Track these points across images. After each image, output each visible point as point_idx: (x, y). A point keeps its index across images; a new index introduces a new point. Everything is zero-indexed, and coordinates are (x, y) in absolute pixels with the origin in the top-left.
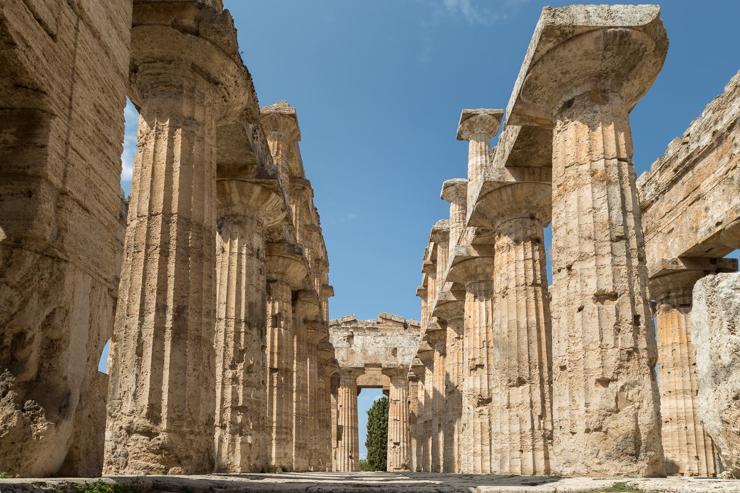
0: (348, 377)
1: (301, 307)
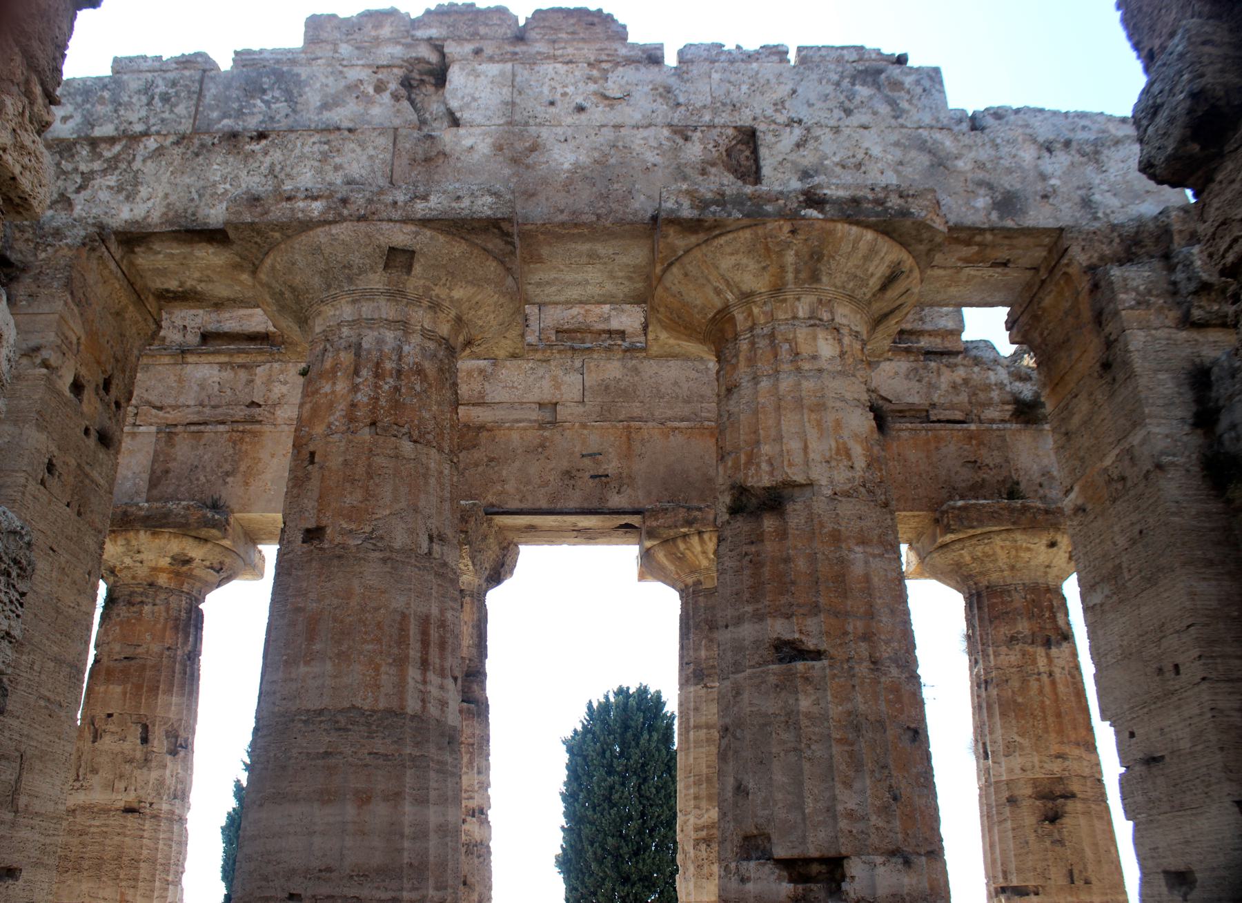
0: (388, 310)
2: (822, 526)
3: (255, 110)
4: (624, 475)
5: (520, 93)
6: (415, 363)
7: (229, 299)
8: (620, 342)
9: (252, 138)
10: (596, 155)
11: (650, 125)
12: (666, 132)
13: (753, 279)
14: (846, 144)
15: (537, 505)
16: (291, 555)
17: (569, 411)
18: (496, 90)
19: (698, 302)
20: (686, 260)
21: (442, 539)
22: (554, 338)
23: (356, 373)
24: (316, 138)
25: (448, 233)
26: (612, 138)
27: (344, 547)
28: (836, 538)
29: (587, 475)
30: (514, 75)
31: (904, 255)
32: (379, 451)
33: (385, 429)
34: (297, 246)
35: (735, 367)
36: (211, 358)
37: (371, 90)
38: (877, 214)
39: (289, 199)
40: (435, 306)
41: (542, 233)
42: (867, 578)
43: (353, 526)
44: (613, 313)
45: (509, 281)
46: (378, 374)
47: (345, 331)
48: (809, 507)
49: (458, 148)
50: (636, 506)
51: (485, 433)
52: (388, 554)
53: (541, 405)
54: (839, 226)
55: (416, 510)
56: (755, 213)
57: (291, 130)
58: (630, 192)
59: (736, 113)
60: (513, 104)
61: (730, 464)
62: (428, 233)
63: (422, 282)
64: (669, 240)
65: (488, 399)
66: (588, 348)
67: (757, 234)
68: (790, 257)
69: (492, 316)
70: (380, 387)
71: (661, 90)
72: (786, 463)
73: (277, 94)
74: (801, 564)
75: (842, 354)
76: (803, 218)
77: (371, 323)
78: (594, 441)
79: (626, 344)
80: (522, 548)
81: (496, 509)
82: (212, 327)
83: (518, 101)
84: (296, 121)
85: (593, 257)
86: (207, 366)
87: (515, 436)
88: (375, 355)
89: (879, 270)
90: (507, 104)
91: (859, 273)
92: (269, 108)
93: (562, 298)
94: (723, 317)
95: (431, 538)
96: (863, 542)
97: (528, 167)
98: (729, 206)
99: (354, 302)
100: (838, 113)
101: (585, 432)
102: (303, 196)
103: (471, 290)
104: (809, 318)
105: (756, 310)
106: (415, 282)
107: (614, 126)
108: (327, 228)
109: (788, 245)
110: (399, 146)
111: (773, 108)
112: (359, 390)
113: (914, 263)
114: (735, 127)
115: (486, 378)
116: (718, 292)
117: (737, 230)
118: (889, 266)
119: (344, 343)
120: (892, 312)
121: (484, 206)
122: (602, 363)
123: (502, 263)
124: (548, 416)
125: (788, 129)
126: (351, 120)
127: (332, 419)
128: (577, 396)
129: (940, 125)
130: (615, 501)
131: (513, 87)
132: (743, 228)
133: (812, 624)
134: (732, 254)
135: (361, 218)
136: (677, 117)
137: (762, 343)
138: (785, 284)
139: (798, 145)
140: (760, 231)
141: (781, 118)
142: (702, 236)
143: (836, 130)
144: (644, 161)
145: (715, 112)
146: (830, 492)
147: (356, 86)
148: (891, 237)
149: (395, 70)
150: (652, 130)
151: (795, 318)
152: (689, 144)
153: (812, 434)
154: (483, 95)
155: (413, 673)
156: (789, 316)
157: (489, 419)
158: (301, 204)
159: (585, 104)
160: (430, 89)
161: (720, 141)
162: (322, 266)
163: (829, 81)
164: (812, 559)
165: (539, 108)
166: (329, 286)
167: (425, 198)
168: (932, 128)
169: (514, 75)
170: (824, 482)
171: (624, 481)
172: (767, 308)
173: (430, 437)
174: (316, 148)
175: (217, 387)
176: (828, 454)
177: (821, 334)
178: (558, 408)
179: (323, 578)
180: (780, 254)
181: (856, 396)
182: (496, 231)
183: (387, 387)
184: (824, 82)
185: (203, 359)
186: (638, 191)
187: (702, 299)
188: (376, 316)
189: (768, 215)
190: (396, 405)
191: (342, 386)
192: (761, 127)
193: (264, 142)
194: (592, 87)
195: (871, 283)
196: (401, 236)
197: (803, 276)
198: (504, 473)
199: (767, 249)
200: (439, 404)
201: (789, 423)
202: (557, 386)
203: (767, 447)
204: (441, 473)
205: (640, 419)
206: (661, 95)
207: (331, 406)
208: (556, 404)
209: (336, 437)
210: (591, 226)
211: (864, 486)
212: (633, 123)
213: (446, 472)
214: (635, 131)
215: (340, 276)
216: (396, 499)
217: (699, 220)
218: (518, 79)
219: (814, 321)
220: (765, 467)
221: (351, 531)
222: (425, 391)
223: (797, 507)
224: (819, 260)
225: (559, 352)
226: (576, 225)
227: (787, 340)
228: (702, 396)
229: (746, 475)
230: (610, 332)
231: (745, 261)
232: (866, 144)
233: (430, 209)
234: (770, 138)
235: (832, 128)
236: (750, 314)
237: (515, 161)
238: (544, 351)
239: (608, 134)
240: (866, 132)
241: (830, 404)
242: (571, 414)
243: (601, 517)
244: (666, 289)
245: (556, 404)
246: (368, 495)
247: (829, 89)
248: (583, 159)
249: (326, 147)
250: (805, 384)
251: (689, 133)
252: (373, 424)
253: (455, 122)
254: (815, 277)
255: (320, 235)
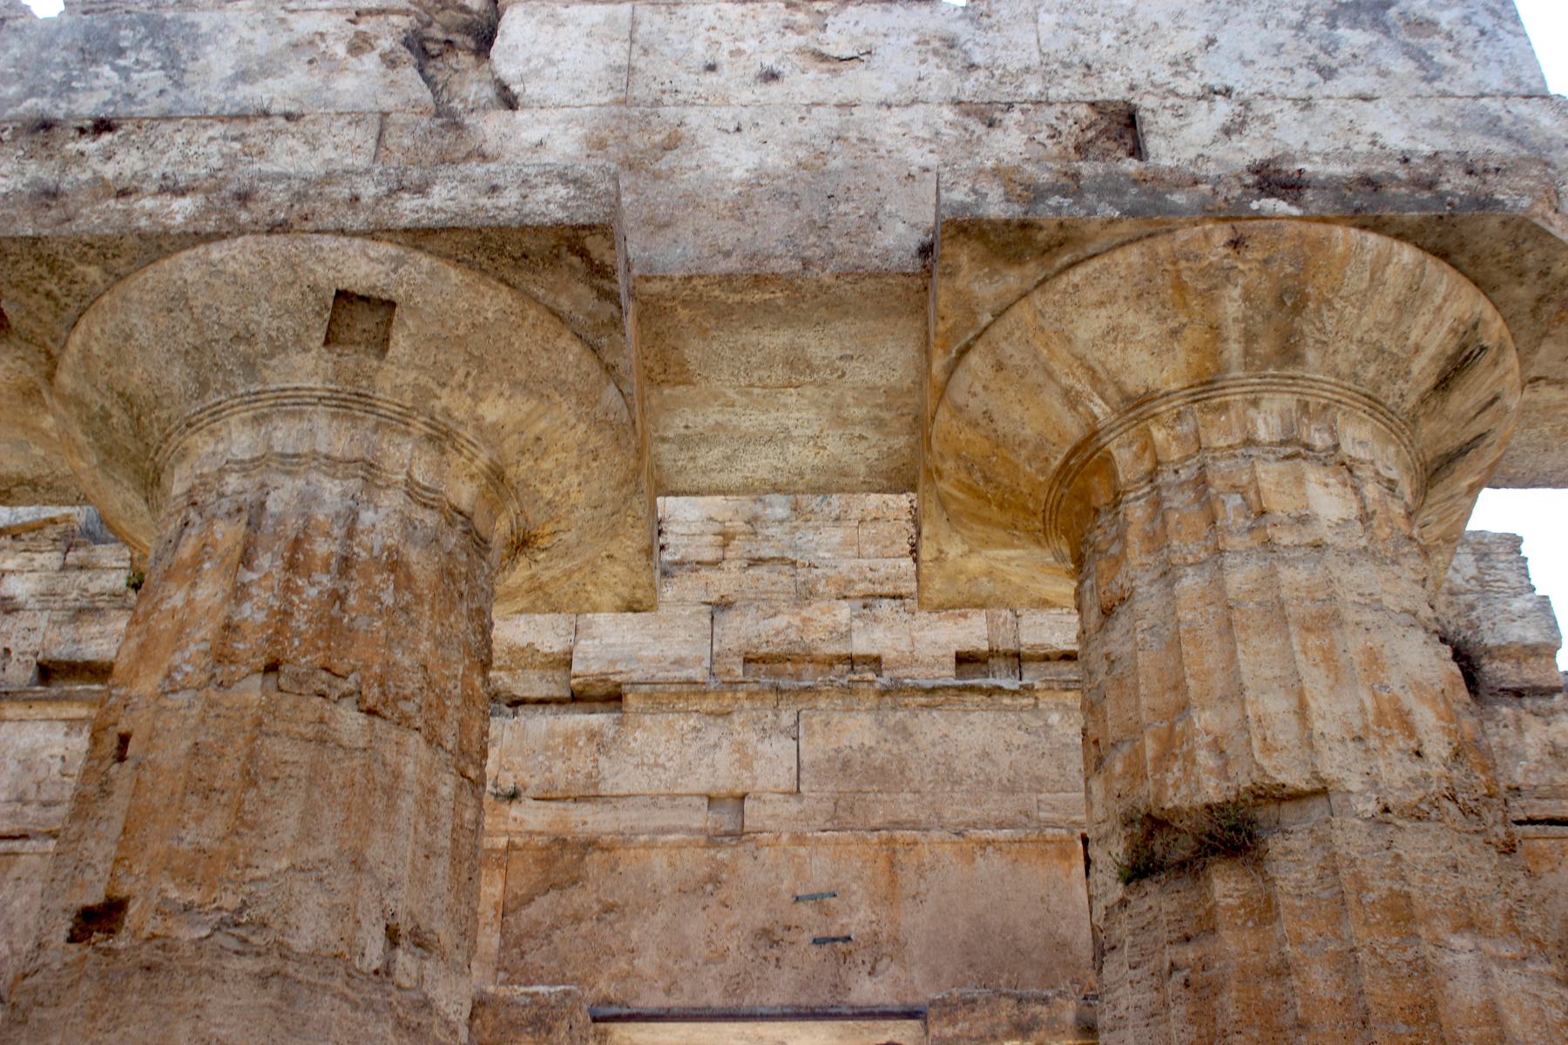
0: (329, 435)
2: (1362, 887)
3: (96, 83)
4: (883, 936)
5: (646, 52)
6: (385, 548)
7: (21, 482)
8: (870, 676)
9: (82, 131)
10: (801, 153)
11: (914, 101)
12: (948, 113)
13: (1151, 365)
14: (1329, 128)
15: (701, 1001)
16: (37, 979)
17: (769, 810)
18: (597, 47)
19: (1028, 432)
20: (997, 332)
21: (422, 943)
22: (740, 671)
23: (246, 560)
24: (218, 129)
25: (471, 266)
26: (835, 125)
27: (165, 944)
28: (1401, 913)
29: (806, 937)
30: (634, 22)
31: (1484, 308)
32: (279, 726)
33: (298, 680)
34: (135, 295)
35: (1118, 561)
36: (51, 710)
37: (340, 50)
38: (1422, 206)
39: (123, 193)
40: (441, 437)
41: (685, 303)
42: (1492, 1014)
43: (195, 896)
44: (858, 623)
45: (610, 394)
46: (292, 566)
47: (233, 482)
48: (1324, 841)
49: (512, 145)
50: (910, 1000)
51: (597, 856)
52: (274, 962)
53: (712, 800)
54: (1339, 231)
55: (358, 864)
56: (1151, 211)
57: (167, 117)
58: (874, 217)
59: (1090, 80)
60: (631, 70)
61: (1119, 767)
62: (426, 261)
63: (411, 376)
64: (960, 283)
65: (605, 789)
66: (808, 689)
67: (1154, 256)
68: (1231, 305)
69: (573, 479)
70: (298, 591)
71: (936, 44)
72: (1256, 744)
73: (146, 56)
74: (1320, 980)
75: (1365, 517)
76: (1258, 216)
77: (290, 462)
78: (820, 869)
79: (884, 680)
81: (614, 1010)
82: (61, 652)
83: (641, 63)
84: (178, 100)
85: (797, 364)
86: (43, 725)
87: (659, 861)
88: (293, 525)
89: (1432, 339)
90: (619, 69)
91: (1388, 343)
92: (127, 79)
93: (735, 479)
94: (1088, 457)
95: (393, 936)
96: (1469, 924)
97: (657, 176)
98: (1090, 198)
99: (258, 420)
100: (1305, 75)
101: (802, 851)
102: (154, 188)
103: (524, 405)
104: (1283, 443)
105: (1159, 434)
106: (397, 373)
107: (838, 106)
108: (201, 249)
109: (1227, 275)
110: (390, 142)
111: (1168, 71)
112: (249, 597)
113: (1505, 333)
114: (1092, 104)
115: (602, 748)
116: (1072, 399)
117: (1111, 249)
118: (1453, 331)
119: (226, 505)
120: (1462, 451)
121: (551, 204)
122: (836, 717)
123: (594, 350)
124: (727, 821)
125: (1204, 104)
126: (294, 100)
127: (177, 658)
128: (786, 780)
129: (1523, 91)
130: (866, 990)
131: (632, 41)
132: (1122, 245)
134: (1101, 304)
135: (278, 228)
136: (970, 87)
137: (1179, 501)
138: (1222, 369)
139: (1227, 132)
140: (1162, 247)
141: (1188, 86)
142: (1032, 270)
143: (1307, 104)
144: (902, 162)
145: (1049, 77)
146: (1372, 807)
147: (311, 43)
148: (1455, 266)
149: (394, 19)
150: (918, 112)
151: (1250, 442)
152: (997, 133)
153: (1315, 680)
154: (568, 55)
156: (1237, 438)
157: (607, 827)
158: (149, 203)
159: (777, 68)
160: (465, 60)
161: (1063, 127)
162: (188, 338)
163: (1280, 22)
164: (1346, 962)
165: (684, 77)
166: (204, 386)
167: (421, 190)
168: (1507, 95)
169: (634, 22)
170: (1355, 784)
171: (882, 949)
172: (1184, 428)
173: (409, 707)
174: (213, 148)
175: (57, 766)
176: (1357, 722)
177: (1313, 475)
178: (748, 804)
179: (102, 1021)
180: (1210, 296)
181: (1407, 604)
182: (575, 260)
183: (313, 592)
184: (1271, 24)
185: (36, 711)
186: (890, 215)
187: (1040, 424)
188: (304, 448)
189: (1176, 210)
190: (332, 628)
191: (209, 591)
192: (1149, 102)
193: (106, 138)
194: (794, 40)
195: (1416, 368)
196: (363, 267)
197: (1263, 347)
198: (634, 934)
199: (1180, 287)
200: (439, 643)
201: (1257, 657)
202: (745, 760)
203: (1207, 714)
204: (433, 791)
205: (915, 825)
206: (936, 52)
207: (180, 630)
208: (743, 798)
209: (181, 698)
210: (787, 282)
211: (1453, 799)
212: (880, 96)
213: (445, 791)
214: (884, 112)
215: (226, 362)
216: (308, 836)
217: (1024, 226)
218: (643, 29)
219: (1294, 449)
220: (1205, 758)
221: (187, 908)
222: (406, 610)
223: (1294, 843)
224: (1297, 309)
225: (751, 695)
226: (758, 281)
227: (1235, 488)
228: (1039, 780)
229: (1161, 785)
230: (851, 660)
231: (1130, 318)
232: (1370, 127)
233: (431, 210)
234: (1166, 120)
235: (1295, 101)
236: (1148, 444)
238: (719, 694)
239: (829, 118)
240: (1369, 106)
241: (1350, 615)
242: (773, 817)
243: (837, 1024)
244: (959, 410)
245: (743, 798)
246: (241, 822)
247: (1284, 35)
248: (775, 159)
249: (237, 146)
250: (1286, 574)
251: (998, 115)
252: (272, 668)
253: (509, 101)
254: (1289, 351)
255: (186, 266)
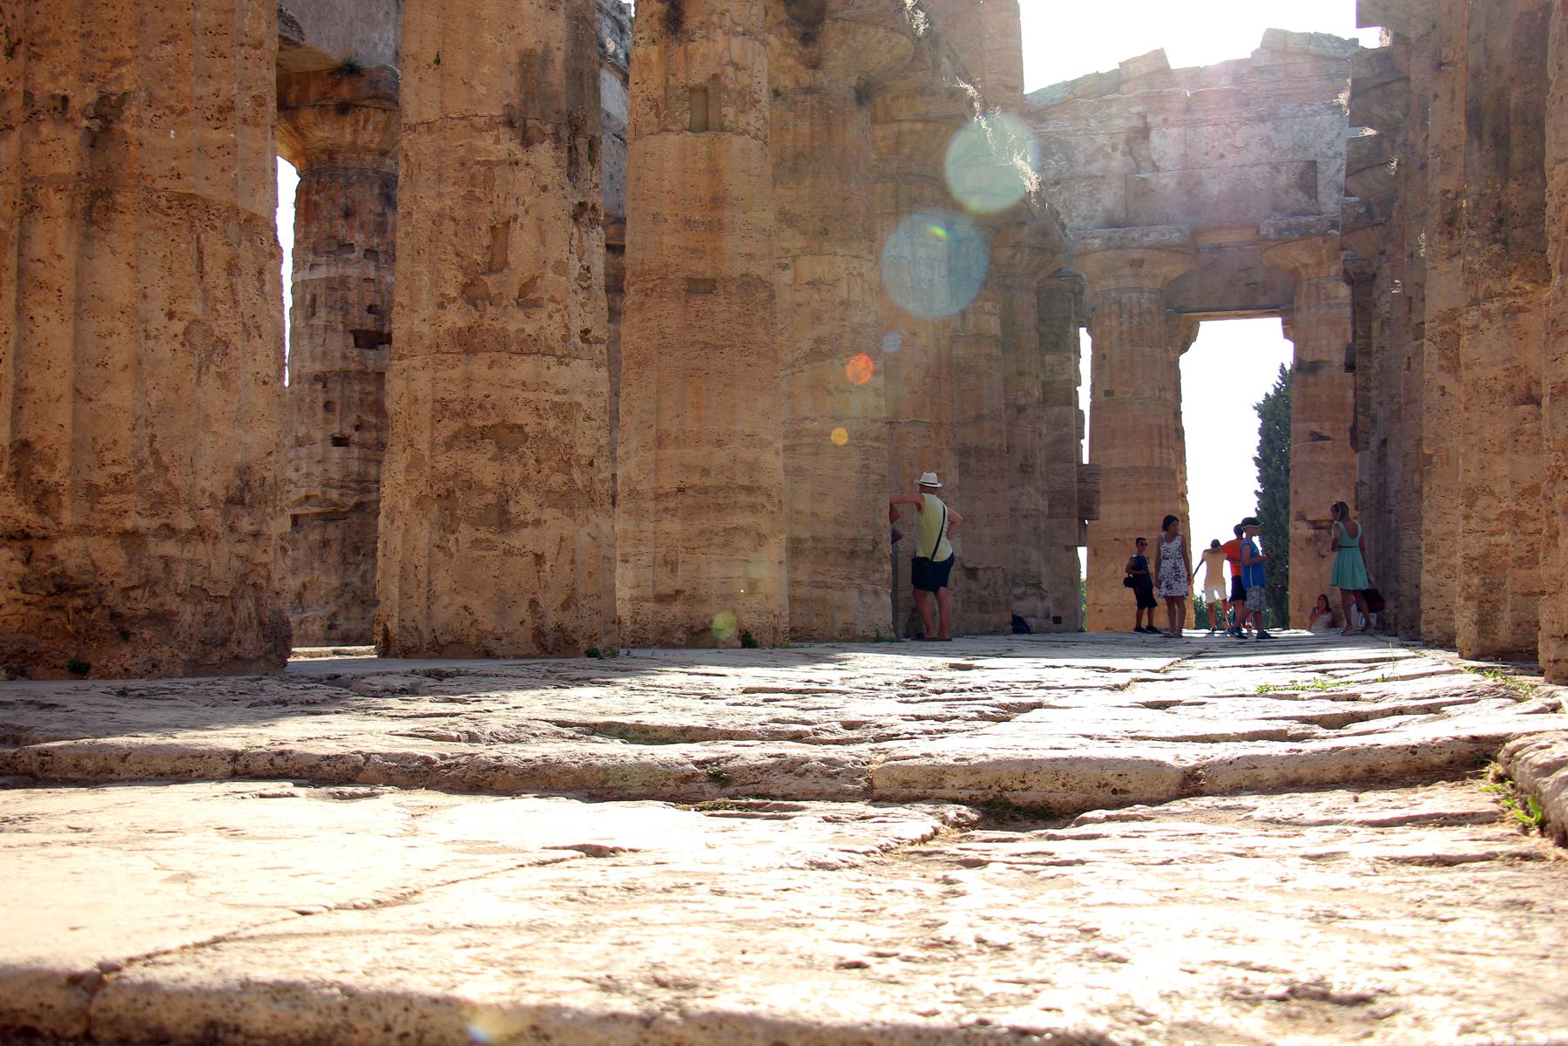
1: (838, 46)
13: (1306, 258)
46: (1131, 317)
68: (1324, 252)
80: (1203, 324)
133: (1327, 425)
135: (1119, 248)
141: (1331, 153)
155: (1157, 450)
191: (1114, 323)
192: (1319, 160)
196: (1138, 254)
237: (1189, 192)
